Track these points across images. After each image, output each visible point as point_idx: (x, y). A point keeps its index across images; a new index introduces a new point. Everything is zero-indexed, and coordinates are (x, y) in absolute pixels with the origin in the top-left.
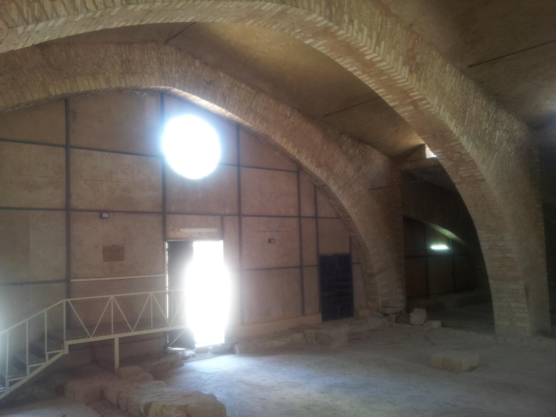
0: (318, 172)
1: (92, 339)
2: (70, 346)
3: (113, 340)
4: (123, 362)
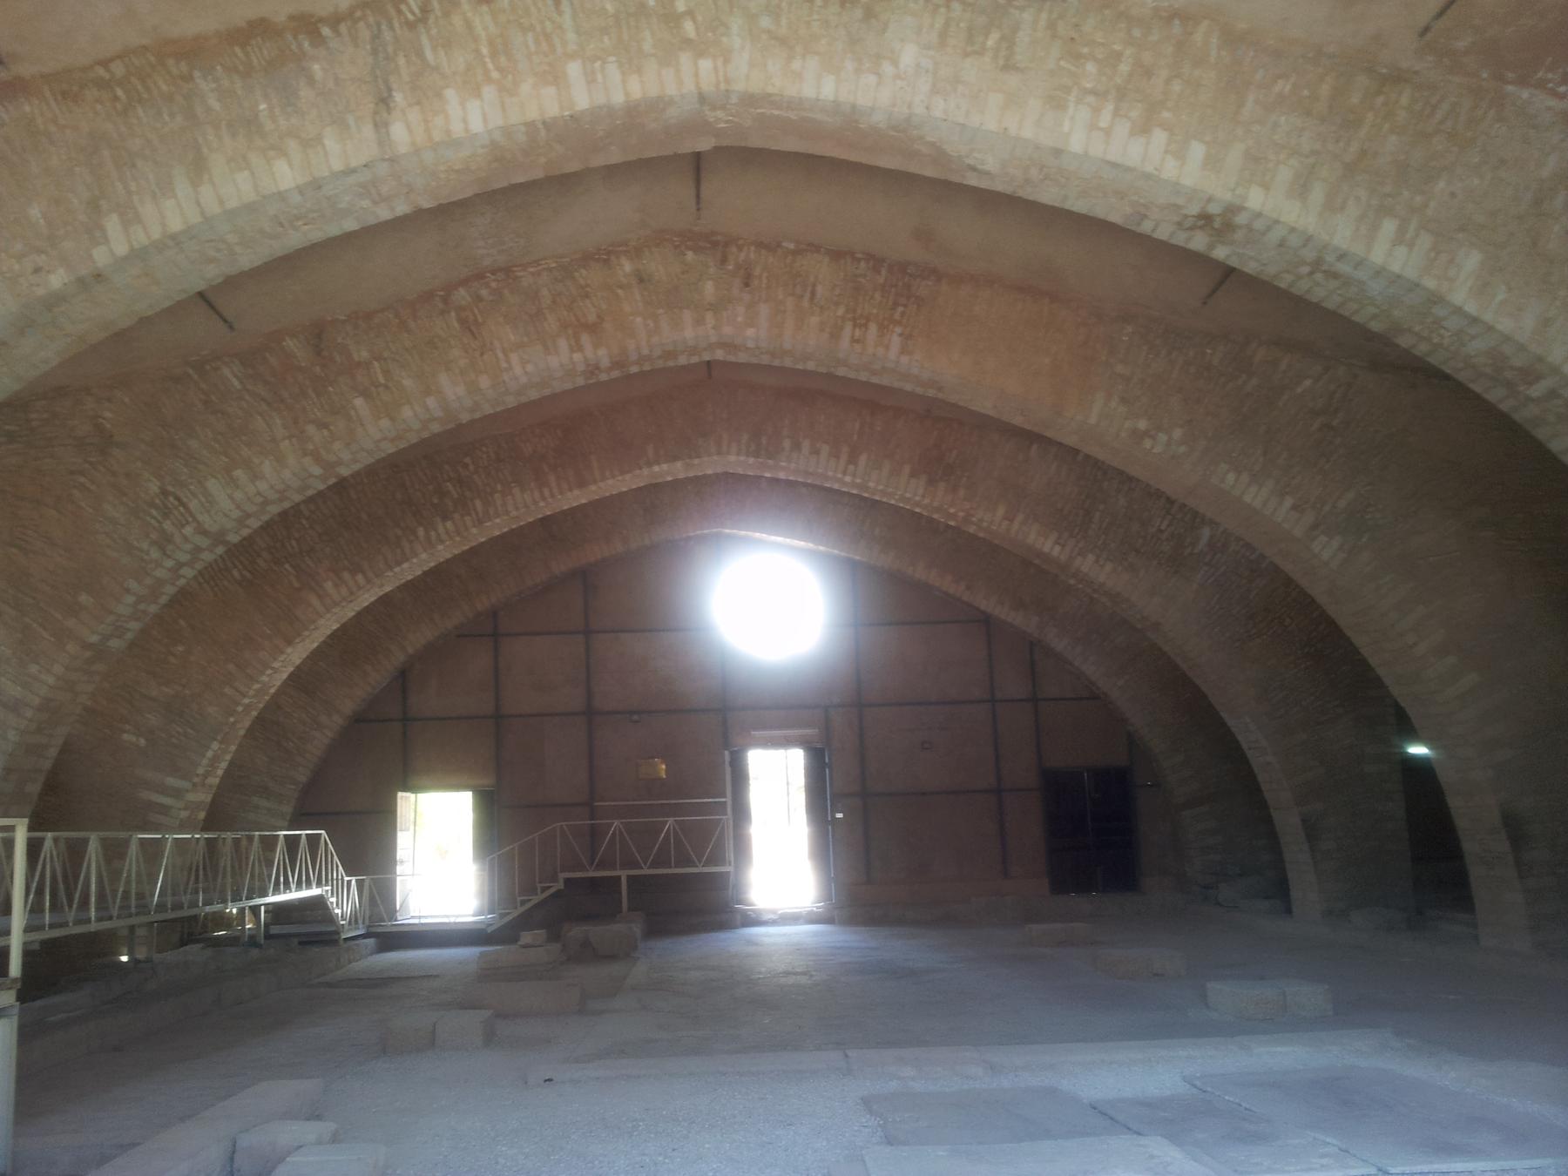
0: (1017, 619)
1: (591, 874)
2: (568, 881)
3: (619, 878)
4: (630, 909)
